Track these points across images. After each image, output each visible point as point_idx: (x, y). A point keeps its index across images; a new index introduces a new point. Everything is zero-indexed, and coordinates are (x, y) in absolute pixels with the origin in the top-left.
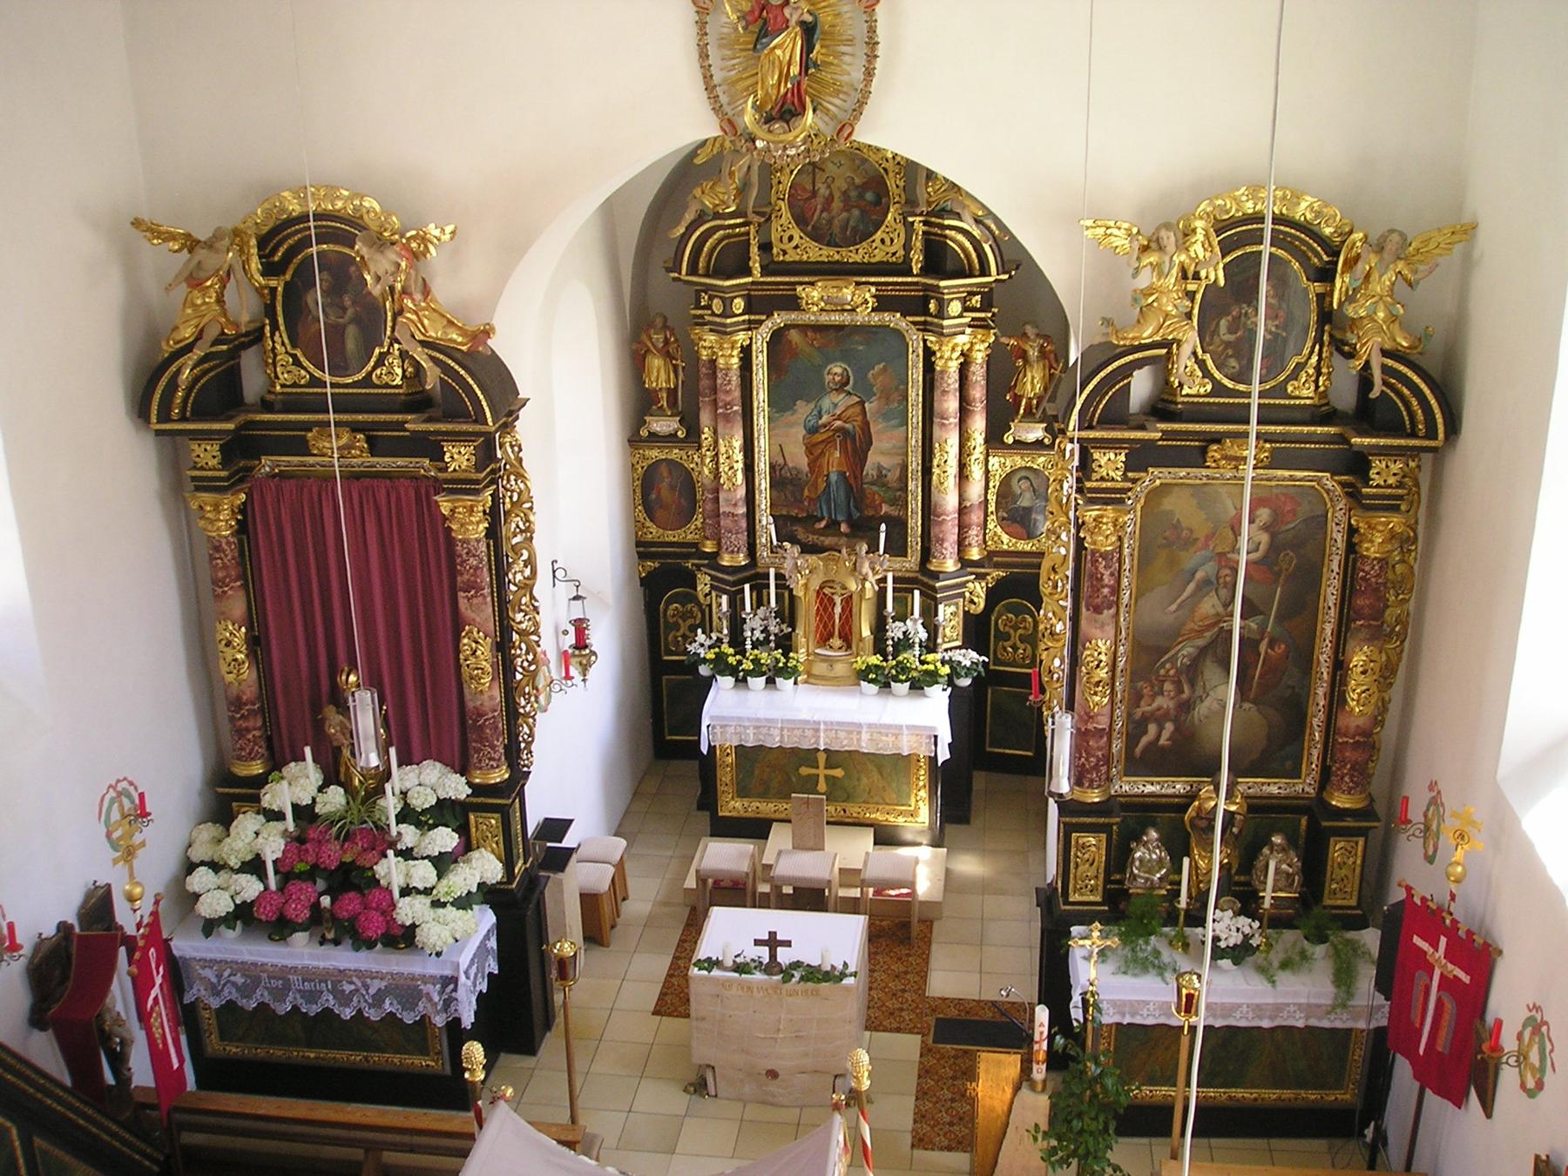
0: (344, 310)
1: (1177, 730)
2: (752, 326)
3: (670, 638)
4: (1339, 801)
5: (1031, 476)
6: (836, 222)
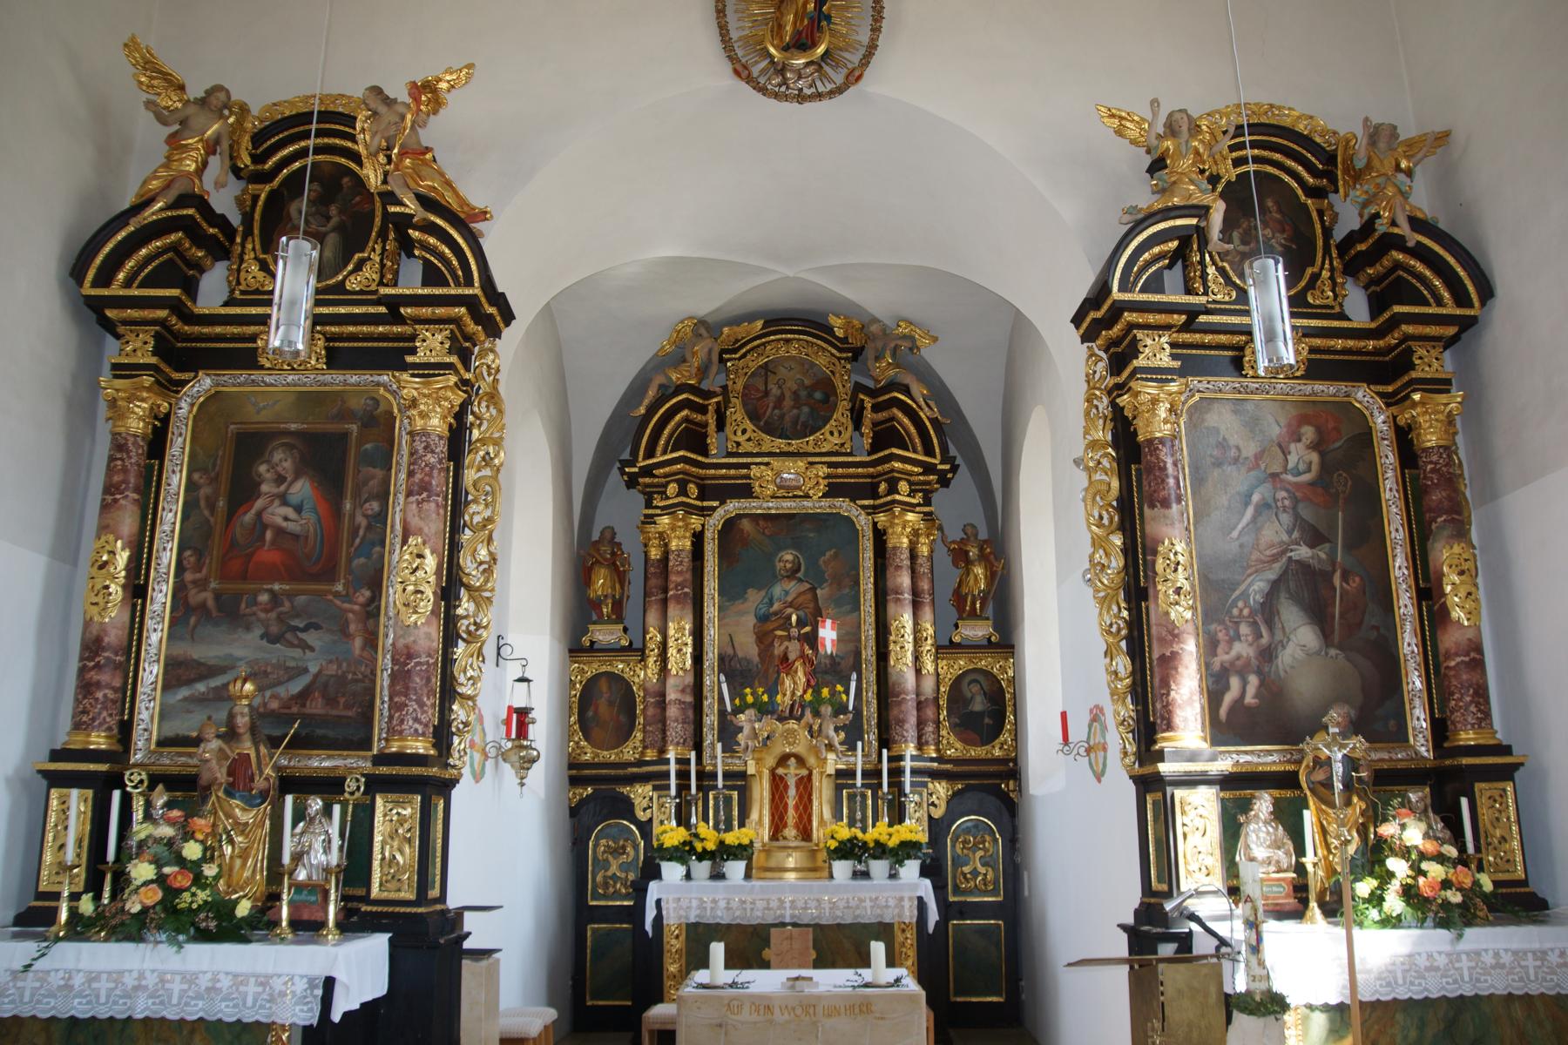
0: (328, 218)
1: (1262, 684)
2: (704, 512)
3: (599, 878)
4: (1468, 737)
5: (981, 678)
6: (787, 418)
